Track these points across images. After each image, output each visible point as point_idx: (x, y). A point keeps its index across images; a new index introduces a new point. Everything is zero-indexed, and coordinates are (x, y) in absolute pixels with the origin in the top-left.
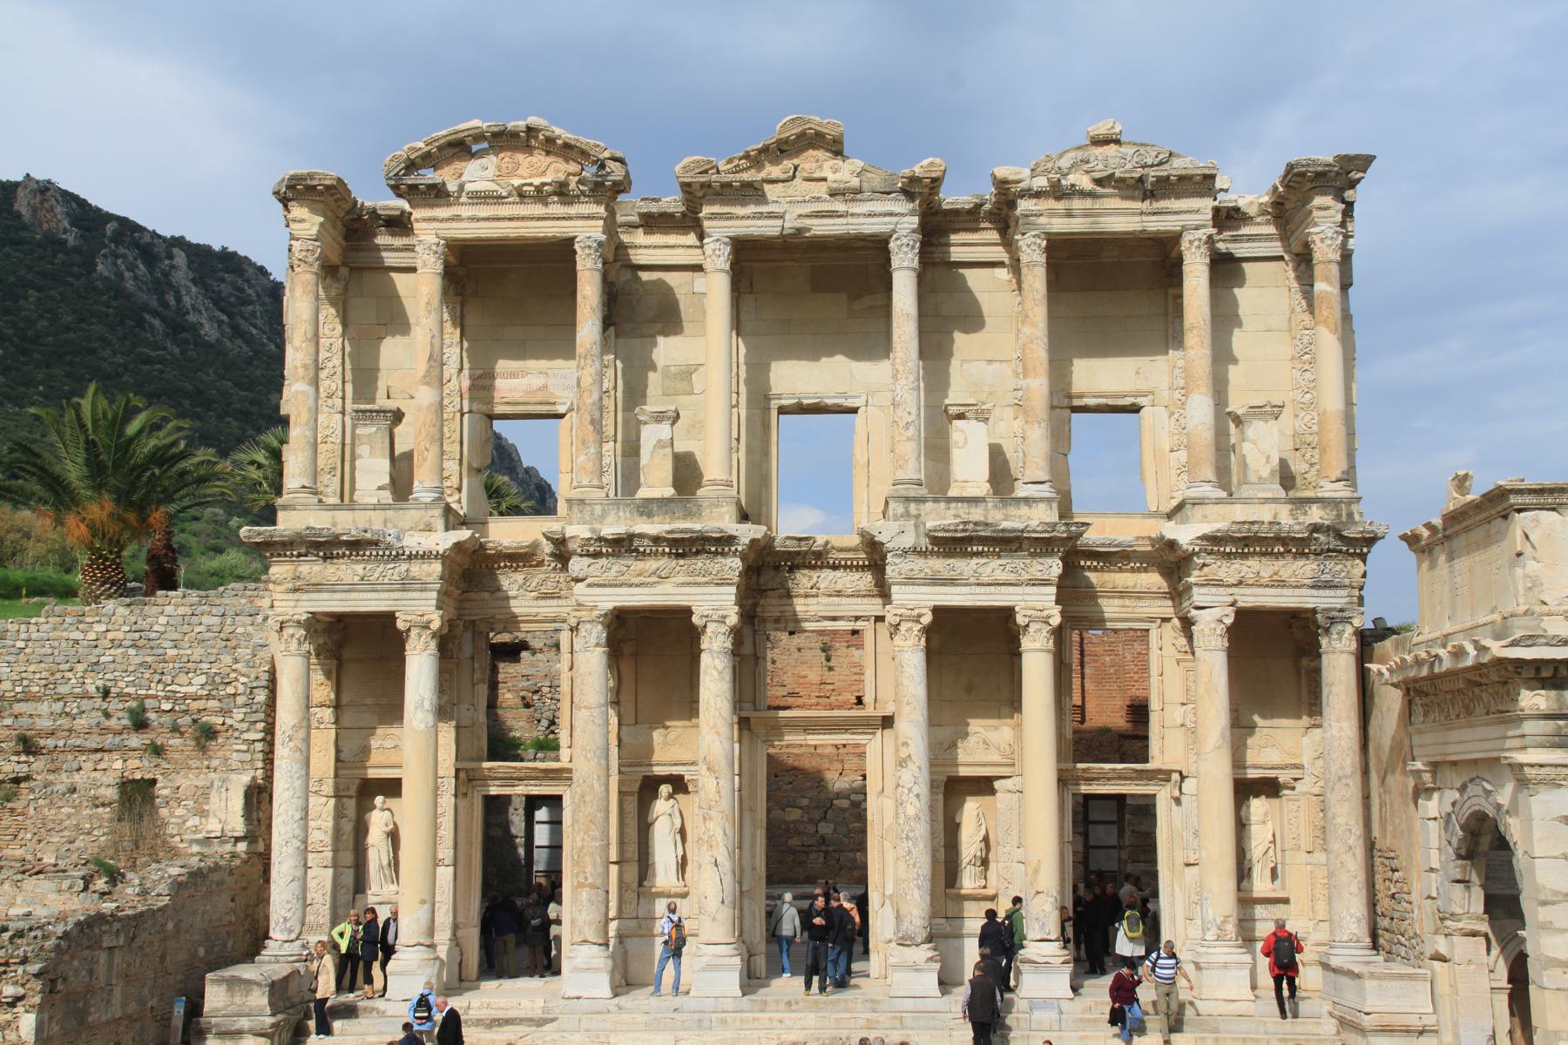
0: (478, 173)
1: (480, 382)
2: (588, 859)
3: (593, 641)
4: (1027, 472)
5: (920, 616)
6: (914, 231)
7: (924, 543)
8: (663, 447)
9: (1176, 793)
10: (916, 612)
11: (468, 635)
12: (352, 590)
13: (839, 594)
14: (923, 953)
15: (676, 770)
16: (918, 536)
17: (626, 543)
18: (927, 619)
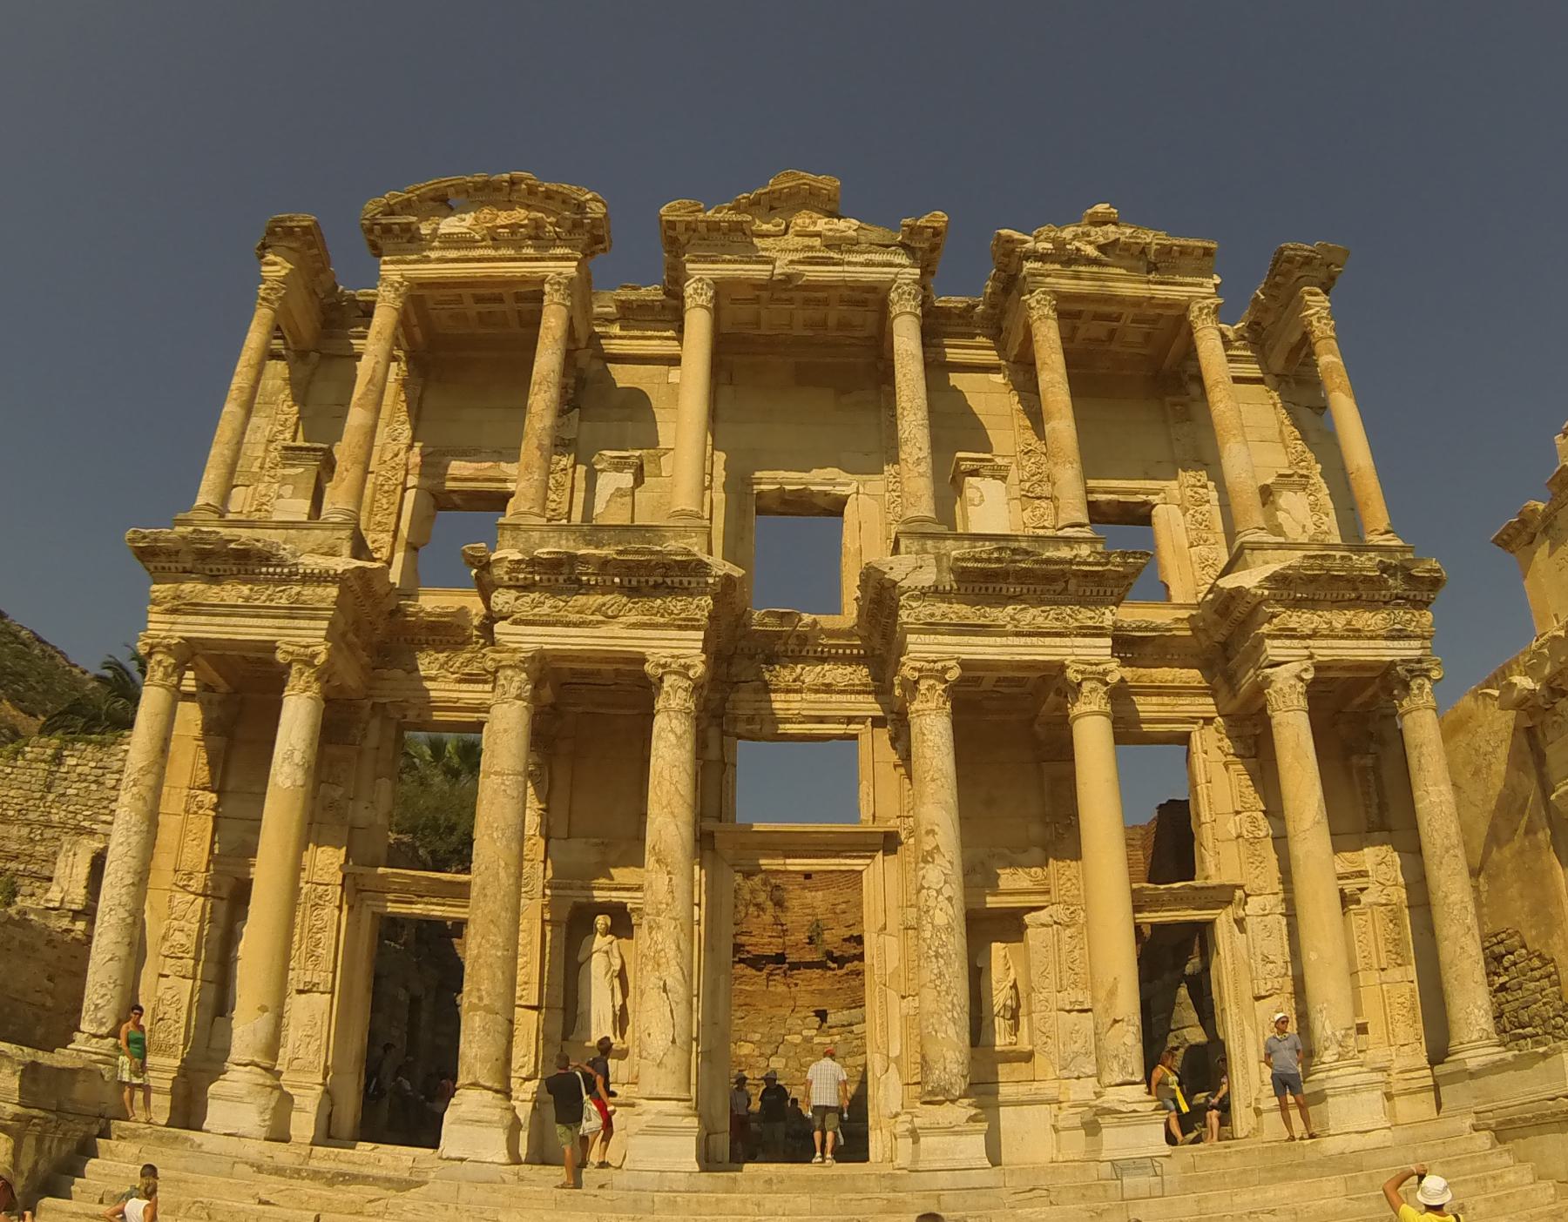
0: (450, 225)
1: (429, 459)
2: (485, 972)
3: (514, 691)
4: (1062, 515)
5: (945, 670)
6: (915, 282)
7: (948, 580)
8: (622, 496)
9: (1241, 913)
10: (939, 666)
11: (375, 725)
12: (232, 617)
13: (828, 689)
14: (960, 1112)
15: (616, 896)
16: (939, 571)
17: (565, 570)
18: (953, 675)
